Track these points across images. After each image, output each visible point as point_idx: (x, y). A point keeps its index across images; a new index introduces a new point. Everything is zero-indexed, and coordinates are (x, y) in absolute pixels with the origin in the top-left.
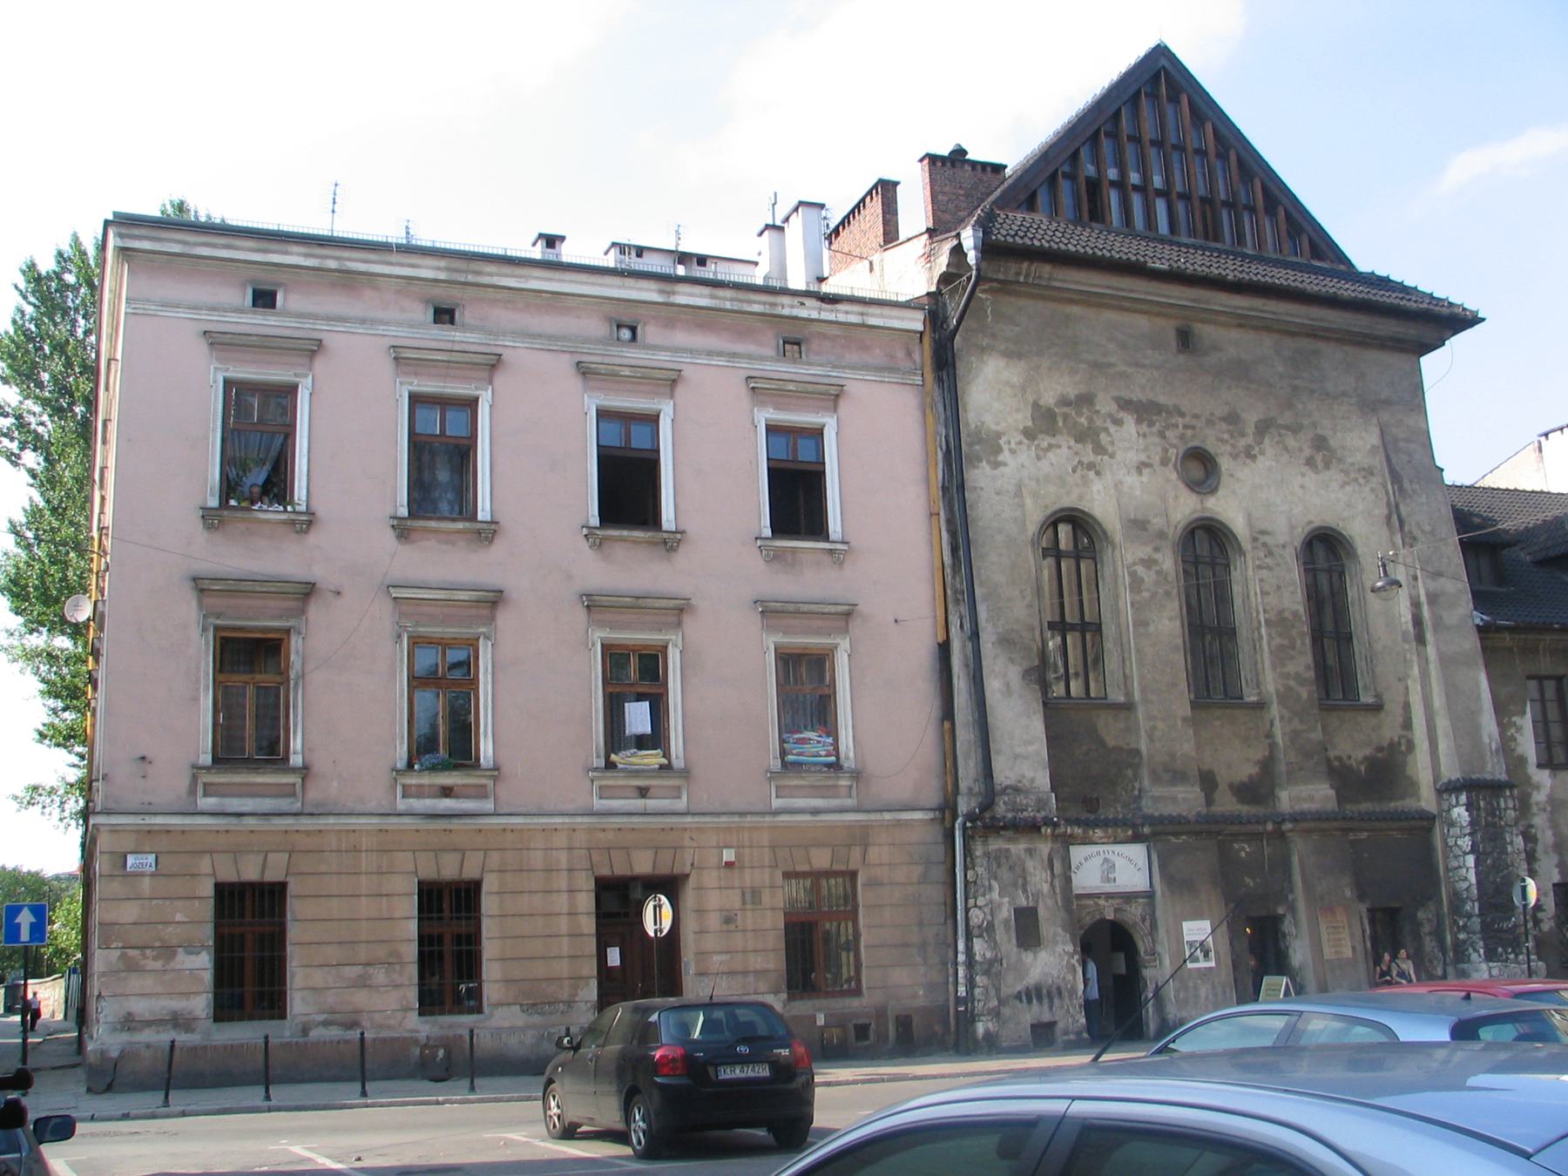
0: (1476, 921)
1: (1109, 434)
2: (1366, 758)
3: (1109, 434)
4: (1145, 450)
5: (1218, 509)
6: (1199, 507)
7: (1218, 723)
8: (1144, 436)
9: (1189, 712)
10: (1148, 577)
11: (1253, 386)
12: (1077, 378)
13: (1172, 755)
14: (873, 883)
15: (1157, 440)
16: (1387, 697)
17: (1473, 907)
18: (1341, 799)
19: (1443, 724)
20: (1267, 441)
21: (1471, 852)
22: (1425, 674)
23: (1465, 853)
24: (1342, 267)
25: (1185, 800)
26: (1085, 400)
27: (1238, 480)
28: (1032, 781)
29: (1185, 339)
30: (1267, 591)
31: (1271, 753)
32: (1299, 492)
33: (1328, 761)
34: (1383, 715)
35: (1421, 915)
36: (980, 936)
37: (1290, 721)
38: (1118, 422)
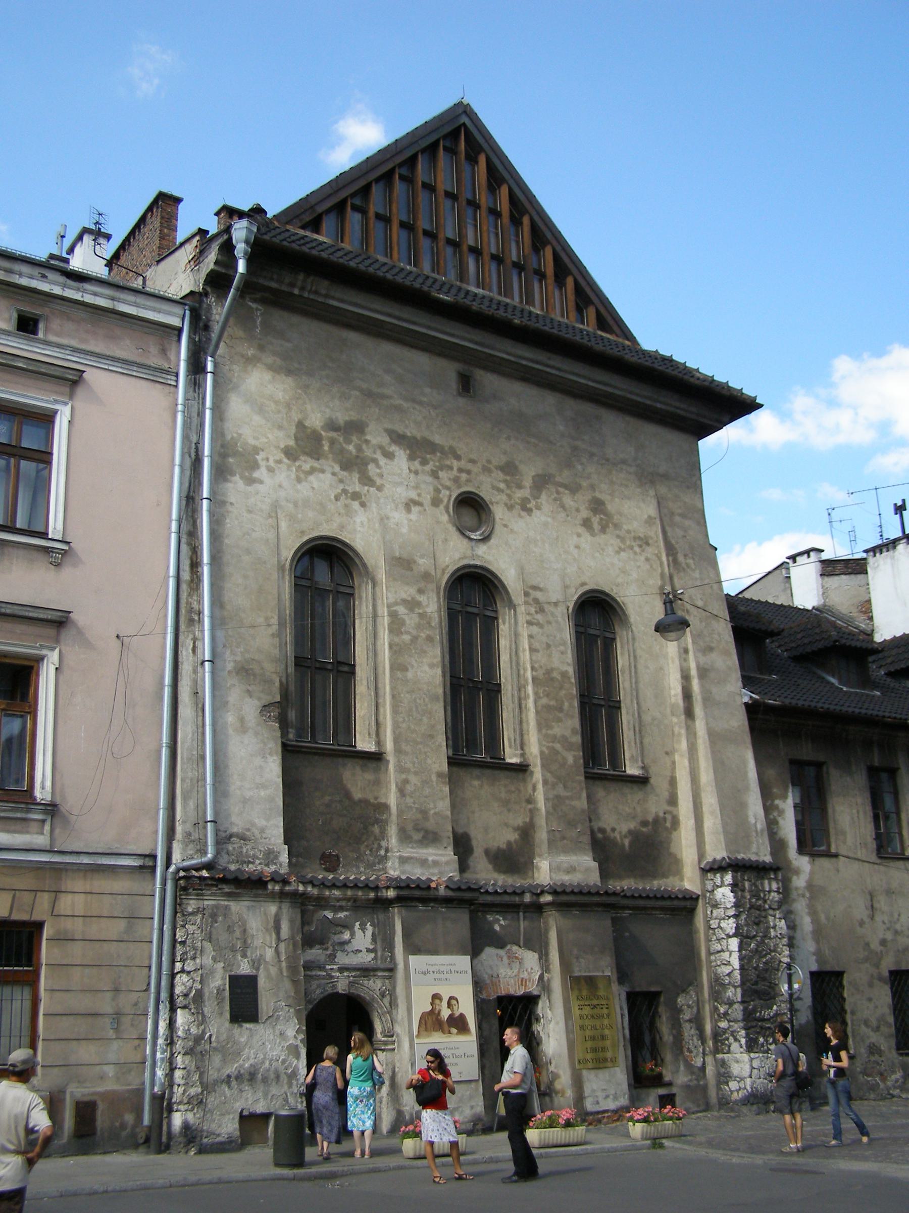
0: (738, 1008)
1: (378, 466)
2: (630, 832)
3: (378, 466)
4: (417, 487)
5: (489, 557)
6: (469, 553)
8: (416, 473)
9: (445, 767)
10: (411, 620)
13: (424, 813)
14: (62, 939)
15: (430, 479)
16: (653, 771)
17: (734, 994)
18: (604, 874)
19: (710, 801)
20: (544, 497)
21: (735, 935)
23: (729, 936)
24: (627, 343)
26: (355, 428)
27: (512, 531)
28: (262, 831)
29: (466, 385)
31: (532, 819)
32: (575, 552)
35: (680, 1000)
36: (184, 1007)
37: (554, 786)
38: (389, 456)
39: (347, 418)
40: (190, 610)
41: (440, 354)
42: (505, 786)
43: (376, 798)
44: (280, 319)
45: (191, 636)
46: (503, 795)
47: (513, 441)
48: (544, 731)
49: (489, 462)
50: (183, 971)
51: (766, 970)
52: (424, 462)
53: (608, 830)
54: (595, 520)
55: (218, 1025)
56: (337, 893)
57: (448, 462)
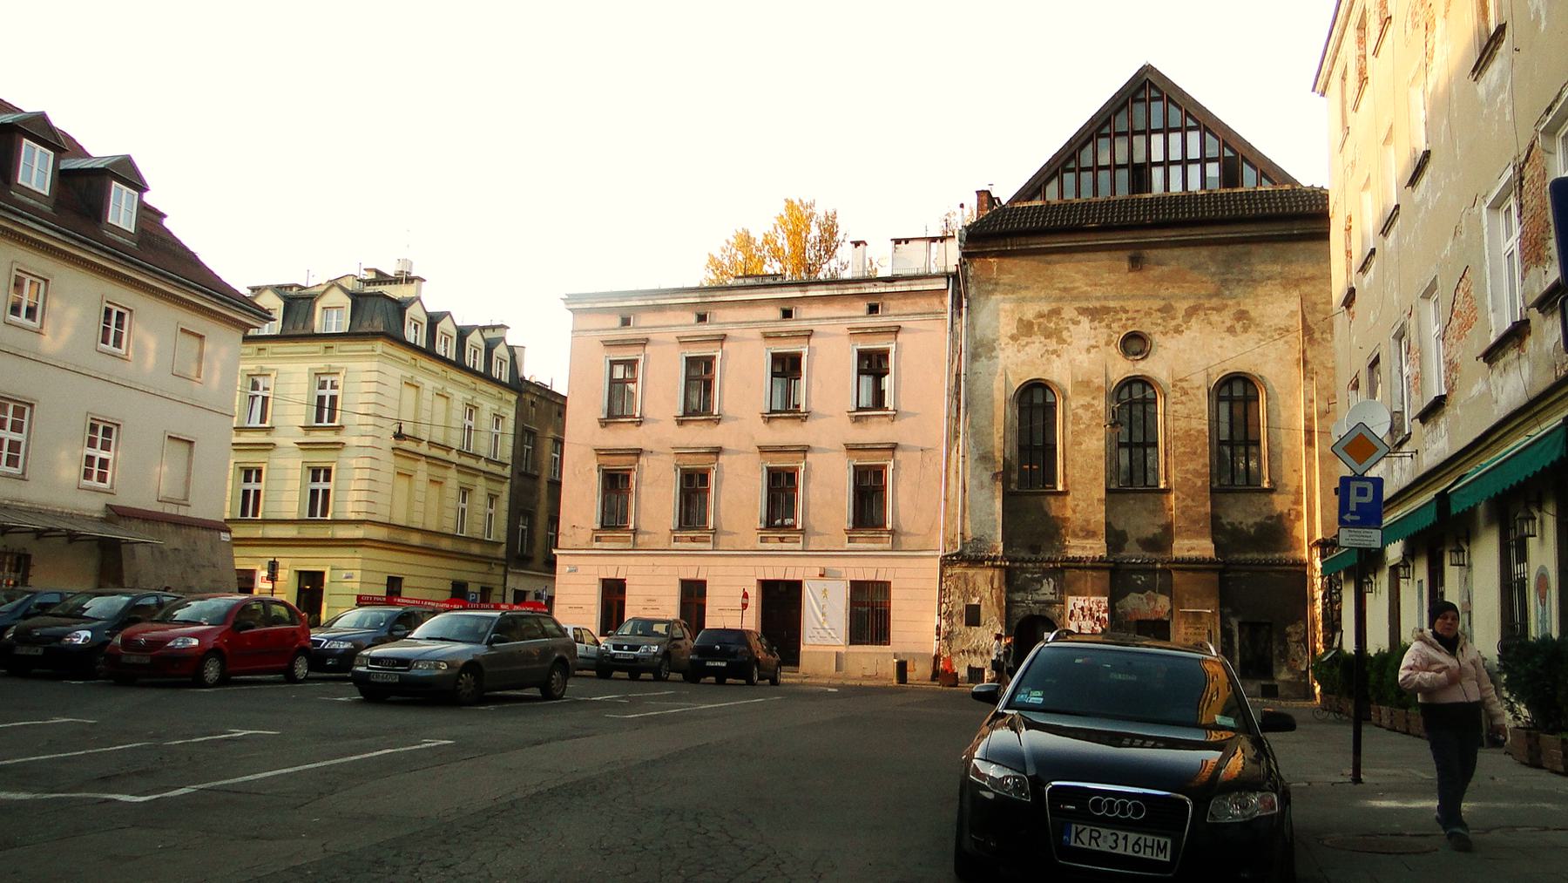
10: (1086, 416)
13: (1088, 521)
22: (1310, 467)
25: (1095, 548)
26: (1056, 312)
29: (1136, 263)
30: (1183, 420)
38: (1077, 323)
52: (1101, 320)
54: (1238, 326)
55: (960, 627)
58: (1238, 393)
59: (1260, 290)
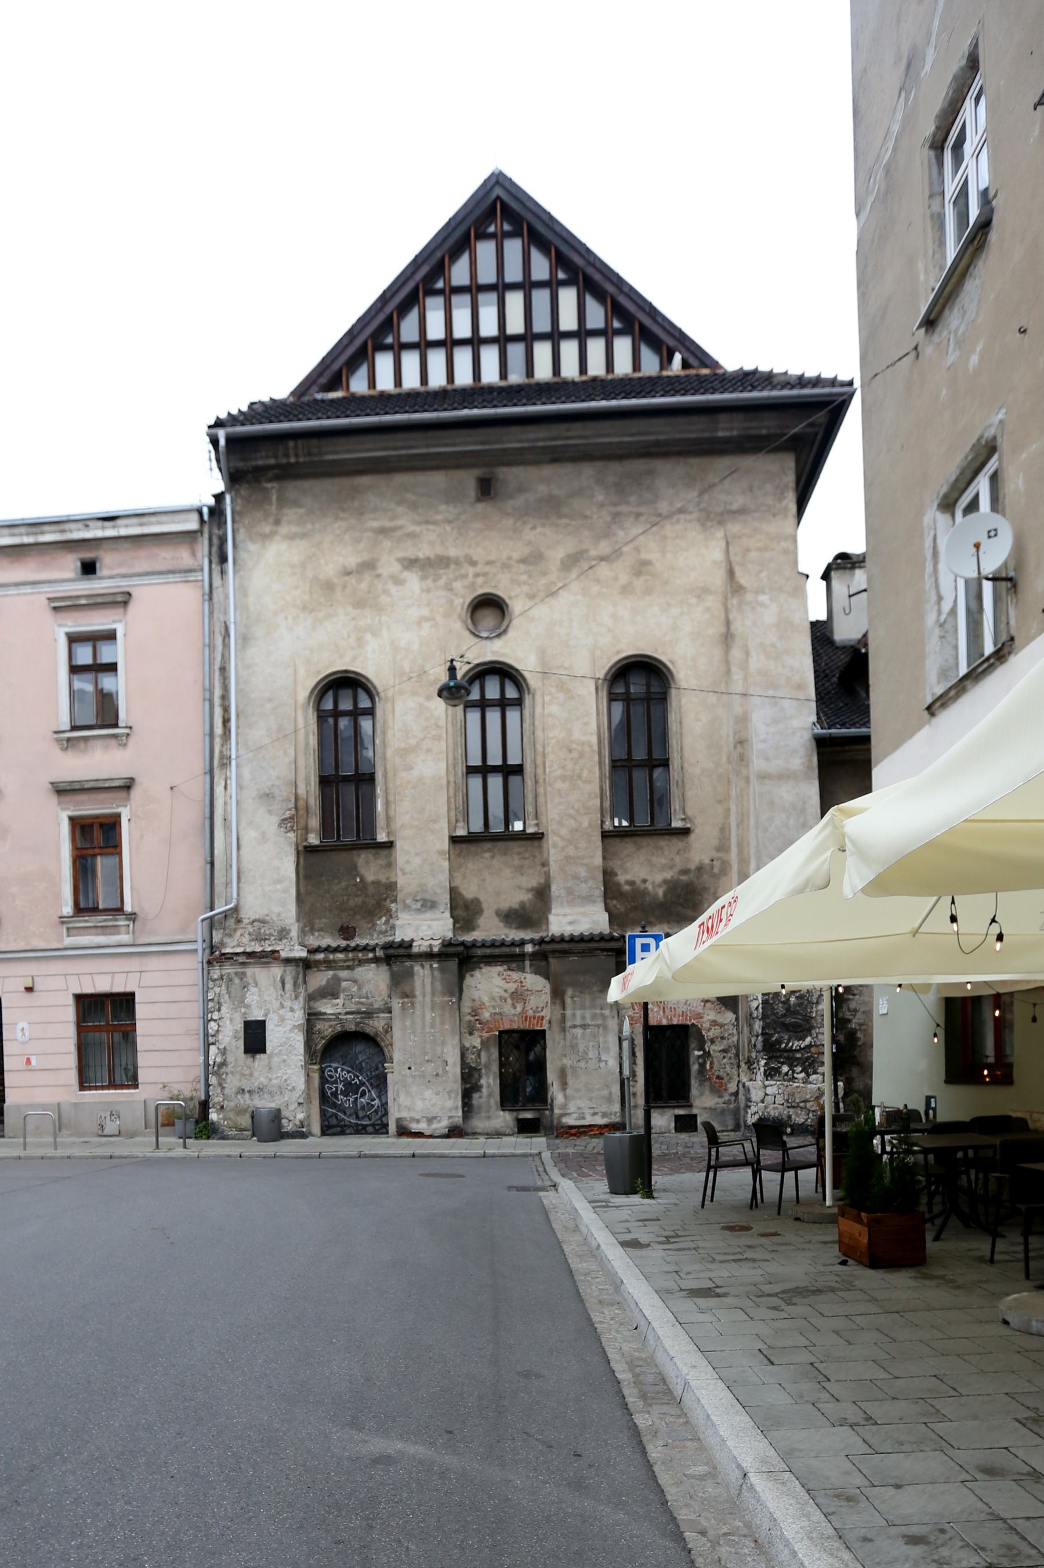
1: (390, 596)
2: (665, 882)
4: (428, 604)
5: (507, 651)
7: (487, 855)
8: (428, 591)
11: (564, 521)
12: (361, 546)
15: (443, 593)
16: (698, 821)
24: (705, 371)
26: (369, 566)
28: (279, 915)
29: (486, 489)
33: (618, 884)
34: (692, 837)
38: (398, 582)
39: (359, 560)
40: (222, 757)
41: (457, 467)
42: (519, 854)
43: (388, 879)
44: (293, 489)
45: (224, 777)
46: (516, 862)
47: (539, 530)
48: (557, 800)
49: (509, 558)
50: (212, 1019)
51: (800, 1005)
53: (638, 882)
54: (639, 583)
56: (340, 956)
57: (463, 571)
58: (639, 685)
59: (669, 529)
